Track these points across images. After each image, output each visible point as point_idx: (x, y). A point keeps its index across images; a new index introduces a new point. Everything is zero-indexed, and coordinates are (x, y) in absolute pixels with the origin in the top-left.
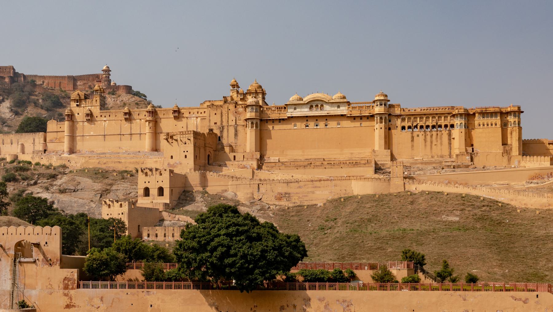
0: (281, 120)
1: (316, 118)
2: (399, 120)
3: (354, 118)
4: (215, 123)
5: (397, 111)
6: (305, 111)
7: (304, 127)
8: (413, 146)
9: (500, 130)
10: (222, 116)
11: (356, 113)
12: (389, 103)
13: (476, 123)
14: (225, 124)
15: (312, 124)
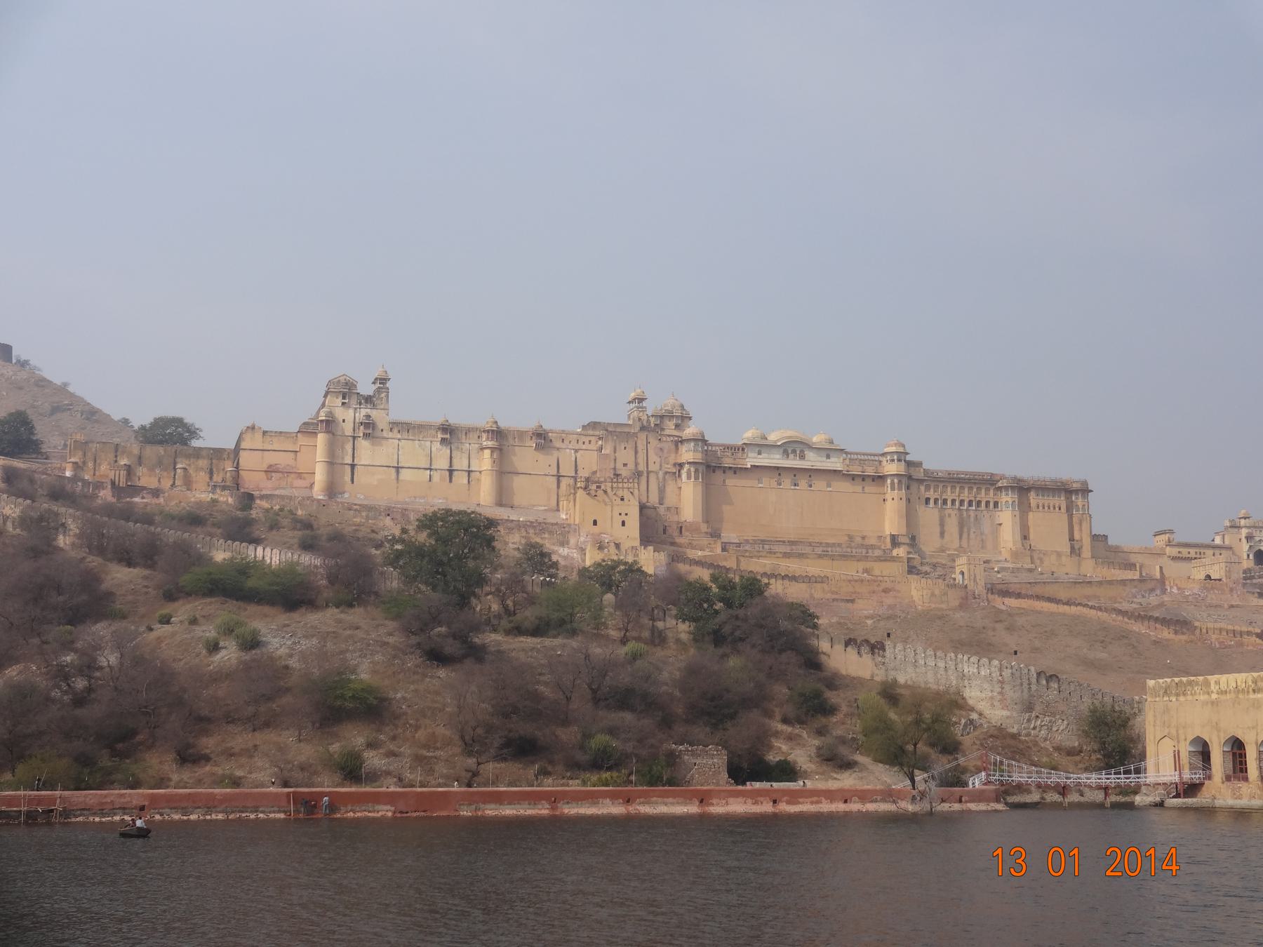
0: (735, 471)
1: (795, 471)
2: (922, 488)
3: (853, 477)
4: (625, 465)
5: (919, 474)
6: (776, 459)
7: (774, 484)
8: (942, 534)
9: (1065, 517)
10: (636, 452)
11: (856, 470)
12: (908, 458)
13: (1033, 503)
14: (642, 467)
15: (787, 482)
